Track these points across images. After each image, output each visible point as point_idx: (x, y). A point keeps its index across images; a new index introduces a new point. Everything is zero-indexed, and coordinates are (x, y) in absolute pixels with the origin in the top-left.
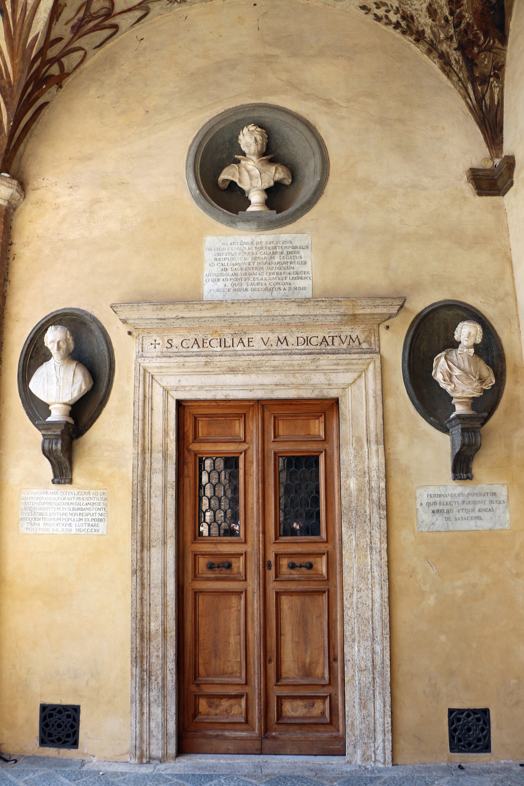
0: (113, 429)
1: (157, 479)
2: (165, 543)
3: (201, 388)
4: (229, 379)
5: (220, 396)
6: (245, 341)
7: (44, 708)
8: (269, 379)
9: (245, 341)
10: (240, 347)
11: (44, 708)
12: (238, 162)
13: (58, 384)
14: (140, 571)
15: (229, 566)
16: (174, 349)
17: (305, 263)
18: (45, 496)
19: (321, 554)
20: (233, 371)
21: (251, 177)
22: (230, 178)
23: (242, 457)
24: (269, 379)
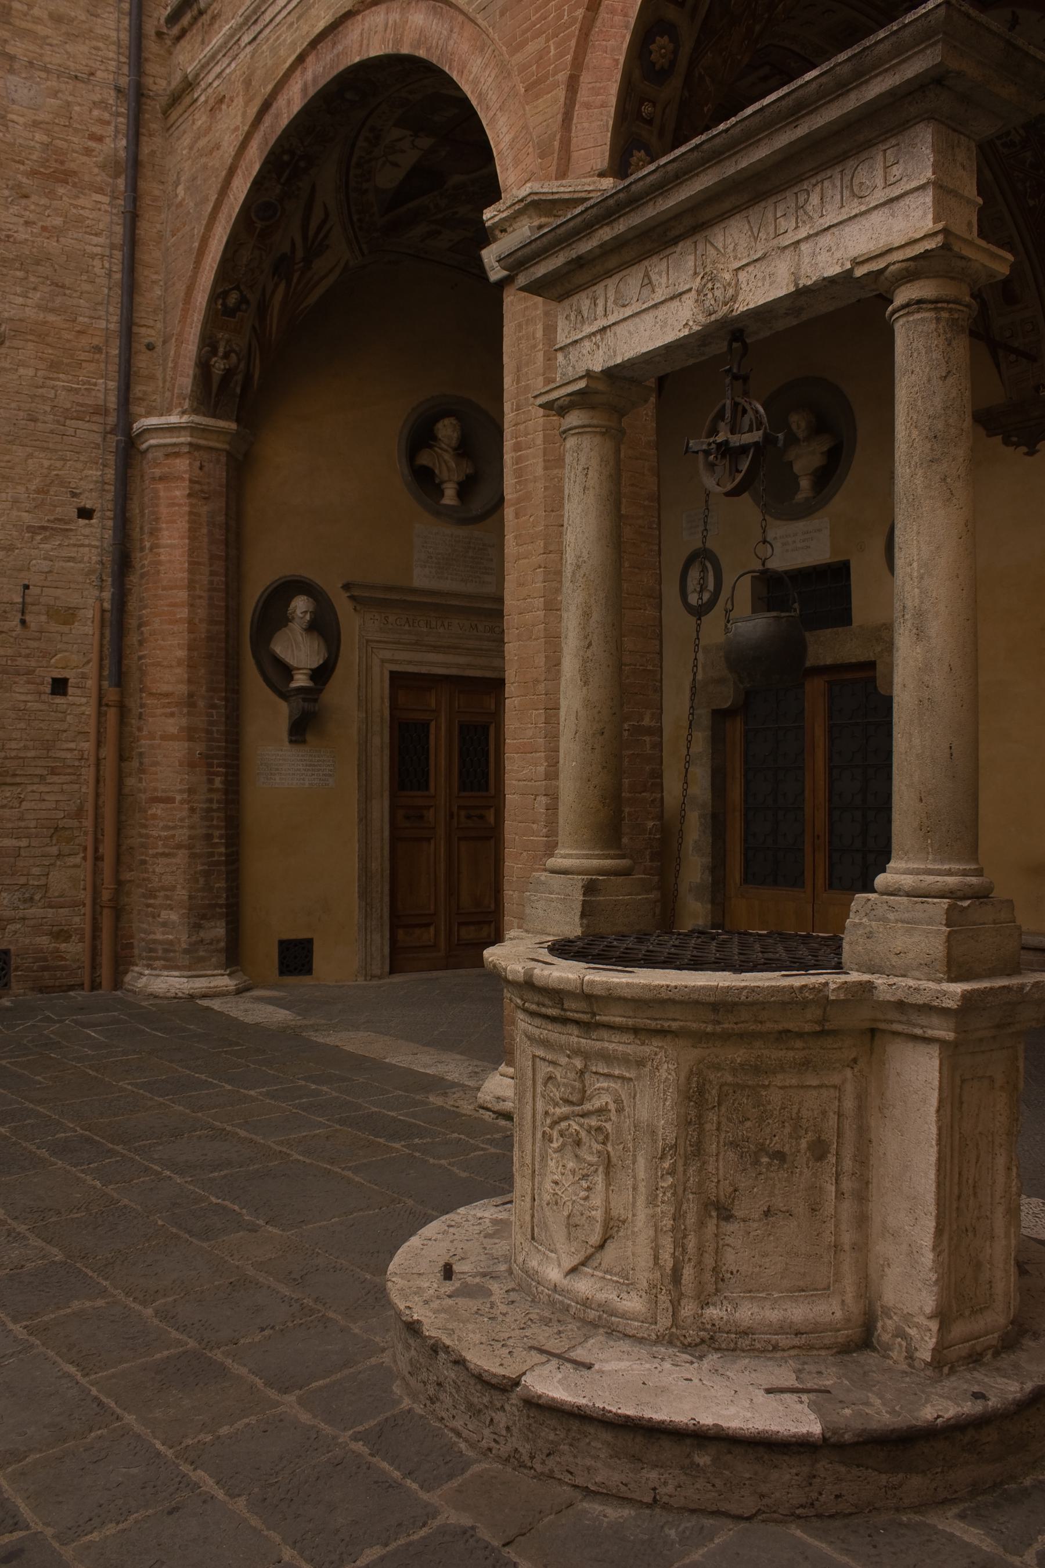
0: (341, 694)
1: (377, 740)
2: (382, 796)
3: (410, 662)
4: (433, 657)
5: (424, 670)
6: (446, 625)
7: (281, 943)
8: (462, 660)
9: (446, 625)
10: (441, 630)
11: (281, 943)
12: (431, 447)
13: (299, 651)
14: (364, 818)
15: (422, 817)
16: (390, 627)
17: (492, 560)
18: (280, 753)
19: (489, 807)
20: (435, 649)
21: (449, 469)
22: (431, 465)
23: (433, 723)
24: (462, 660)
